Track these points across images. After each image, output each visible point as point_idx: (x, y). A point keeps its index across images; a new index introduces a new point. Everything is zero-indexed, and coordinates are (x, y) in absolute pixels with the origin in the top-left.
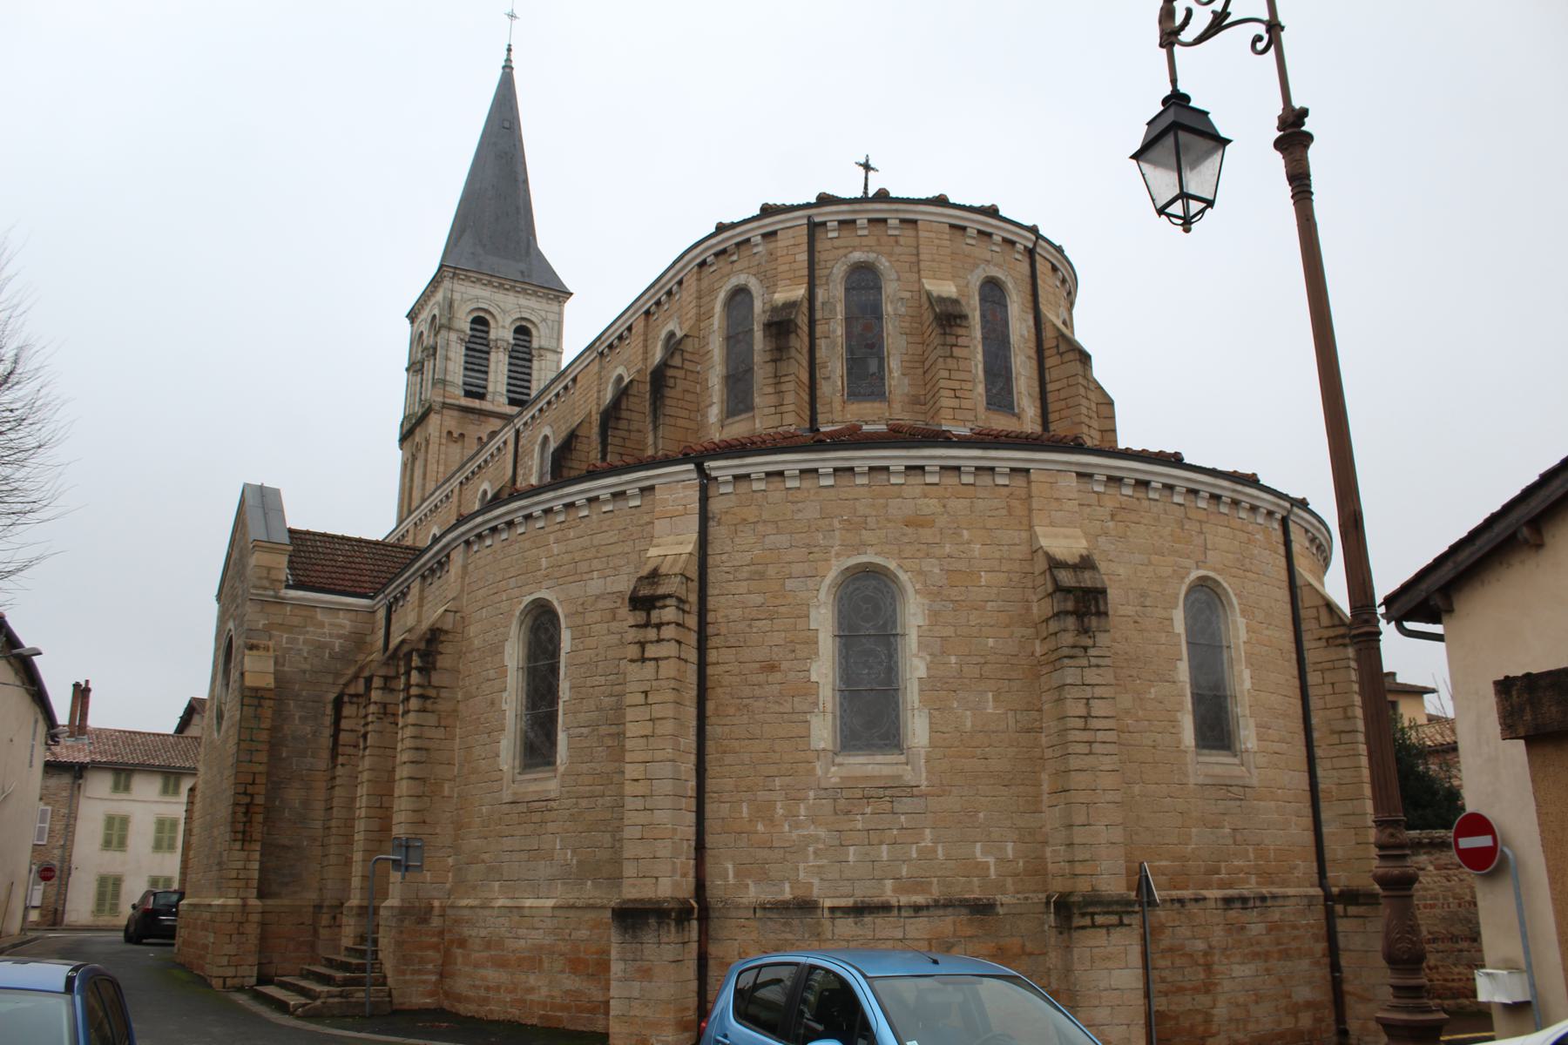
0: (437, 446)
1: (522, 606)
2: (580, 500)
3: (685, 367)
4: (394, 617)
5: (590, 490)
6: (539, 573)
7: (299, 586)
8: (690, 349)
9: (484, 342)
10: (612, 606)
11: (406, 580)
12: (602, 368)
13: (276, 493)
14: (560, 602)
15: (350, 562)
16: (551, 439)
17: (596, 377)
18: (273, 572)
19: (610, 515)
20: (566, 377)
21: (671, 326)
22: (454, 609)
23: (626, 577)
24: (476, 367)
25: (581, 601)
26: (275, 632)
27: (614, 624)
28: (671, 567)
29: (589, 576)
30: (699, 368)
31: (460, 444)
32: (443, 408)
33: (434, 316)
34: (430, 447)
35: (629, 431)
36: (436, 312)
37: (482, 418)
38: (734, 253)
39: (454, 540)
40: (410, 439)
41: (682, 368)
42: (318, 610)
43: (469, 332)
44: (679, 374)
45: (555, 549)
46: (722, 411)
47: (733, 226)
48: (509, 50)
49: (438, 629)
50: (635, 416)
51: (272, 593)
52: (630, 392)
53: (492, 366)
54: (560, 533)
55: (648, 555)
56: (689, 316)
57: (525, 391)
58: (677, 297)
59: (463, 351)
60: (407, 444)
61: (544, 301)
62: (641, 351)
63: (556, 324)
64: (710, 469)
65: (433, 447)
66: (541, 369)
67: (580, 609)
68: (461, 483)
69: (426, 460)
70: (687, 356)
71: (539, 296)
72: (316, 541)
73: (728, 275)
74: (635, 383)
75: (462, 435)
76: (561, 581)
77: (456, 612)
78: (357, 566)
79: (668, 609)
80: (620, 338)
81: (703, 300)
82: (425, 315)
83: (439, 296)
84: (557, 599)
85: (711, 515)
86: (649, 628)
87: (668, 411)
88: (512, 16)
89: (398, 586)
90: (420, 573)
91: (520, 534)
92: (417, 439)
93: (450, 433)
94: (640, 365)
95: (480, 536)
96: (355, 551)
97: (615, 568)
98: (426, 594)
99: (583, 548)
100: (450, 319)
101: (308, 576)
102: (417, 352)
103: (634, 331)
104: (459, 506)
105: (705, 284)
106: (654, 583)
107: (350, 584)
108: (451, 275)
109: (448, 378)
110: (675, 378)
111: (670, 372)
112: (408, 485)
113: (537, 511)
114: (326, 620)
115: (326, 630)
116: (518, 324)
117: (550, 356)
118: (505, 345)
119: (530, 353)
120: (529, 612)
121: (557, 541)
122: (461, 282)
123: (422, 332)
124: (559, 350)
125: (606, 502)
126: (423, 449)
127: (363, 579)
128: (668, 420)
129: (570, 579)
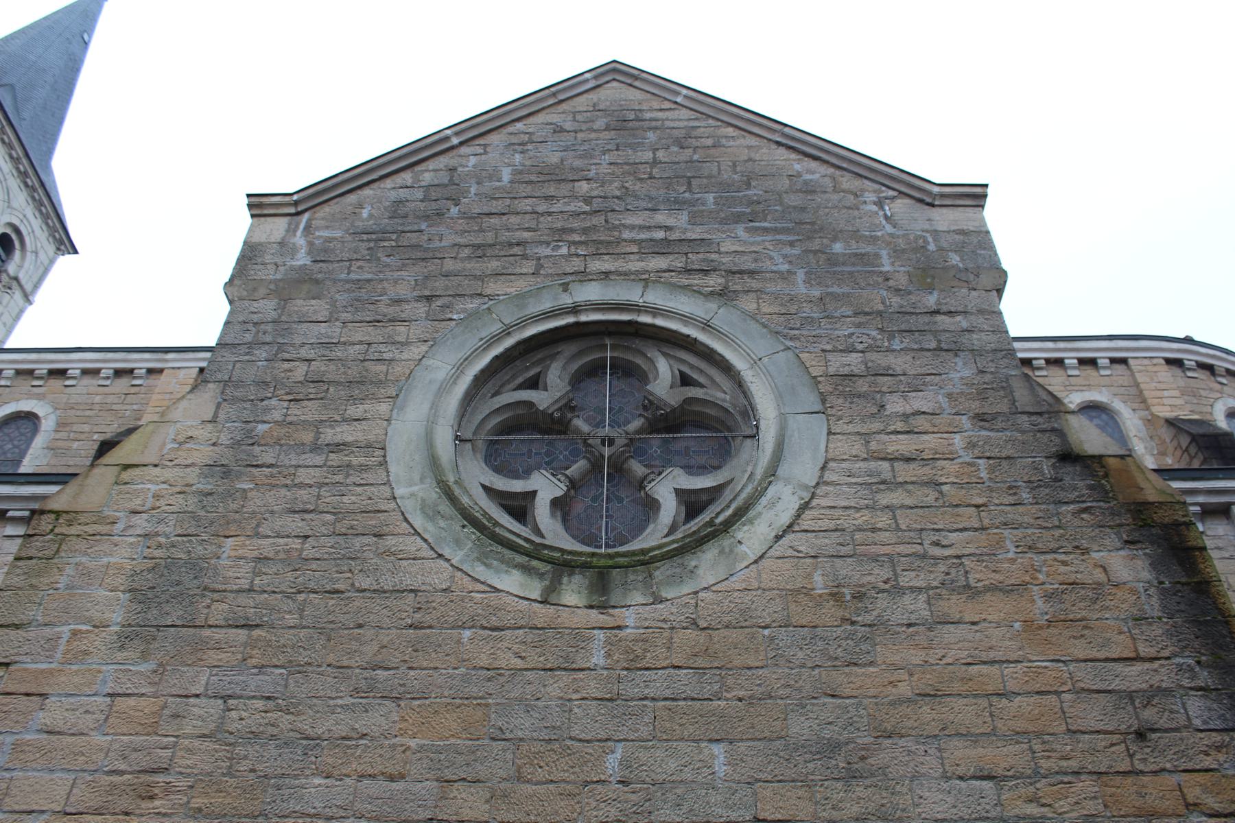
61: (46, 234)
71: (47, 224)
117: (18, 295)
124: (31, 298)
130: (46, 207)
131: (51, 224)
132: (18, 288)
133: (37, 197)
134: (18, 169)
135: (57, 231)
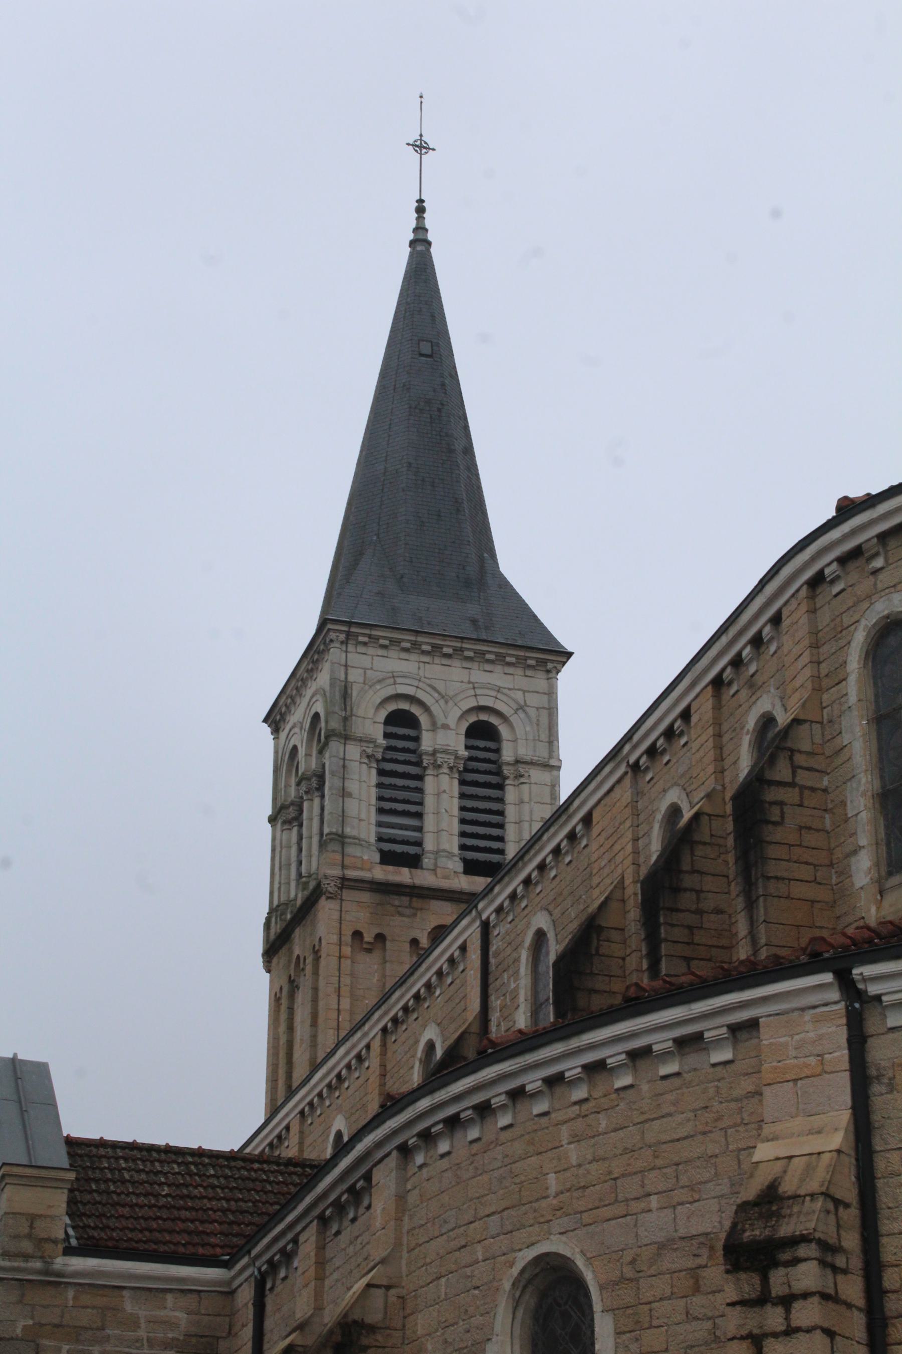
0: (334, 961)
1: (515, 1271)
2: (614, 1055)
3: (798, 780)
4: (269, 1300)
5: (633, 1035)
6: (544, 1203)
7: (87, 1249)
8: (806, 746)
9: (412, 758)
10: (690, 1264)
11: (290, 1227)
12: (638, 793)
13: (41, 1070)
14: (589, 1260)
15: (182, 1197)
16: (551, 935)
17: (628, 811)
18: (38, 1223)
19: (677, 1082)
20: (570, 817)
21: (765, 704)
22: (385, 1283)
23: (713, 1205)
24: (400, 807)
25: (628, 1256)
26: (46, 1342)
27: (697, 1300)
28: (802, 1180)
29: (642, 1205)
30: (825, 782)
31: (377, 955)
32: (341, 888)
33: (316, 716)
34: (323, 963)
35: (700, 912)
36: (319, 707)
37: (417, 903)
38: (876, 555)
39: (379, 1145)
40: (283, 951)
41: (793, 785)
42: (125, 1293)
43: (381, 741)
44: (789, 795)
45: (573, 1153)
46: (877, 865)
47: (870, 501)
48: (420, 210)
49: (355, 1322)
50: (709, 883)
51: (38, 1265)
52: (696, 837)
53: (429, 801)
54: (579, 1124)
55: (755, 1159)
56: (798, 683)
57: (495, 845)
58: (773, 648)
59: (374, 778)
60: (279, 960)
61: (519, 671)
62: (711, 755)
63: (544, 714)
64: (865, 980)
65: (328, 964)
66: (522, 802)
67: (629, 1272)
68: (384, 1030)
69: (315, 989)
70: (800, 759)
71: (509, 664)
72: (117, 1159)
73: (869, 597)
74: (705, 820)
75: (380, 938)
76: (586, 1218)
77: (388, 1288)
78: (198, 1204)
79: (802, 1267)
80: (670, 734)
81: (824, 649)
82: (299, 715)
83: (323, 678)
84: (583, 1253)
85: (873, 1072)
86: (768, 1307)
87: (772, 869)
88: (421, 147)
89: (276, 1240)
90: (316, 1212)
91: (505, 1128)
92: (297, 951)
93: (357, 935)
94: (710, 784)
95: (427, 1137)
96: (191, 1174)
97: (691, 1188)
98: (329, 1253)
99: (626, 1151)
100: (346, 719)
101: (105, 1227)
102: (287, 786)
103: (694, 719)
104: (383, 1075)
105: (824, 618)
106: (771, 1215)
107: (183, 1239)
108: (342, 637)
109: (348, 831)
110: (781, 804)
111: (771, 794)
112: (283, 1040)
113: (533, 1082)
114: (142, 1313)
115: (142, 1333)
116: (472, 719)
117: (536, 775)
118: (452, 762)
119: (499, 773)
120: (529, 1282)
121: (576, 1139)
122: (361, 649)
123: (295, 748)
124: (553, 762)
125: (665, 1056)
126: (309, 969)
127: (209, 1228)
128: (772, 886)
129: (607, 1212)
130: (489, 652)
131: (513, 660)
132: (527, 767)
133: (471, 654)
134: (424, 652)
135: (526, 658)
